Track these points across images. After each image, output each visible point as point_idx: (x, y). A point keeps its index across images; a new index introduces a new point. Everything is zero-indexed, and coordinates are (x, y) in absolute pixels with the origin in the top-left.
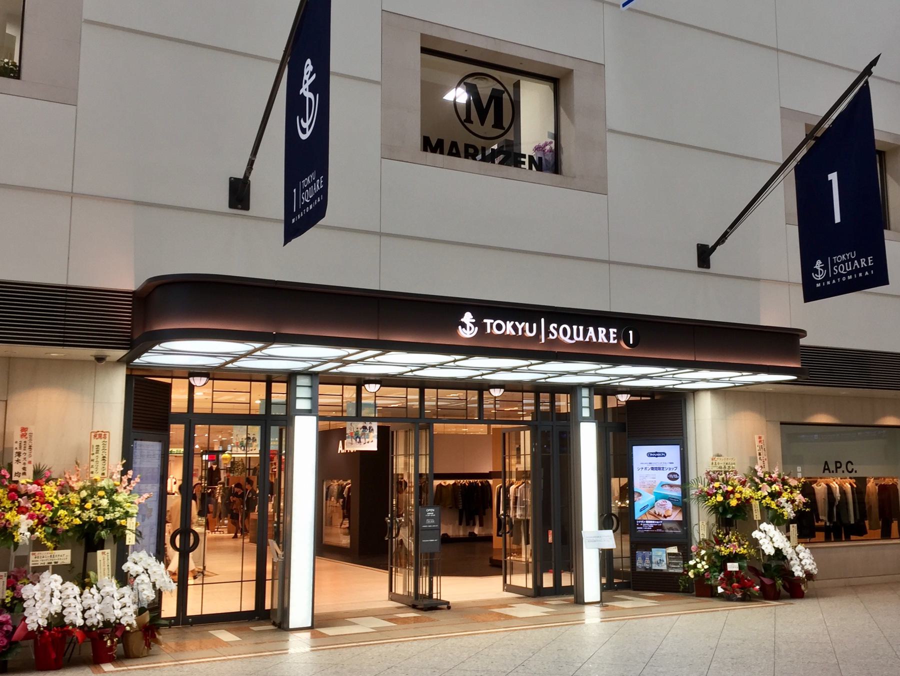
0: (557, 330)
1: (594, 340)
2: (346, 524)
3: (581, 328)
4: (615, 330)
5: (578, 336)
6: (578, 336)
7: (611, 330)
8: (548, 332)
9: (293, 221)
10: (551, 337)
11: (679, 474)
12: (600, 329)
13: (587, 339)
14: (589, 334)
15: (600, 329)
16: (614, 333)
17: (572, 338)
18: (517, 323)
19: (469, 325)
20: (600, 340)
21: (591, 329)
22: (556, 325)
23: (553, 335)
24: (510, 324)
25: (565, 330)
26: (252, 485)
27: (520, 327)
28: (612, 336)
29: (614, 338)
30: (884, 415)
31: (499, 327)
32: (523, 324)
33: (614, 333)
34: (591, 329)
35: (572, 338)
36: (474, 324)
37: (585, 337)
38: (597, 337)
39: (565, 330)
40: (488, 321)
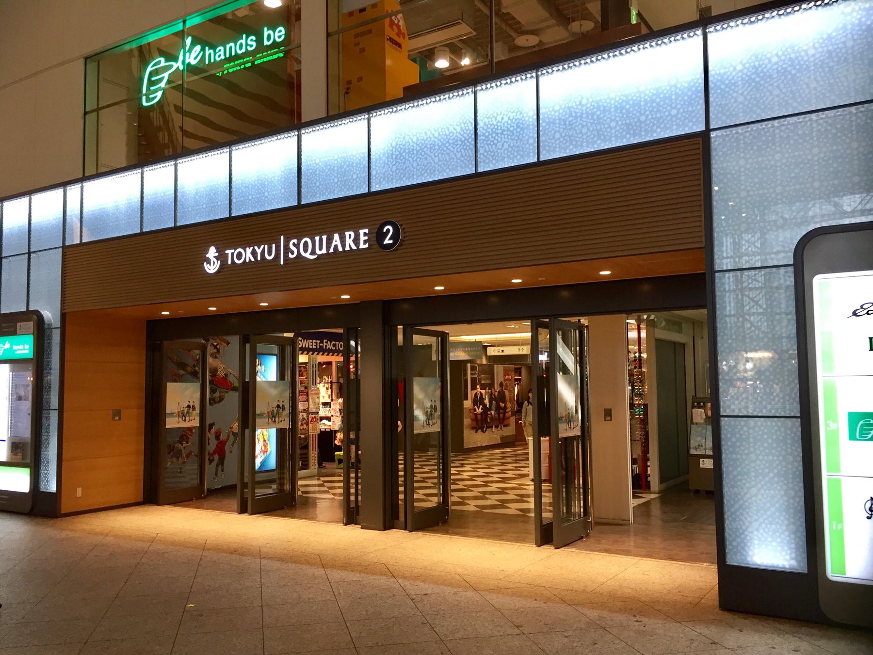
0: (297, 246)
1: (340, 249)
2: (341, 400)
3: (324, 237)
4: (367, 231)
5: (321, 249)
6: (321, 249)
7: (362, 232)
8: (287, 250)
9: (466, 62)
10: (291, 256)
11: (208, 356)
12: (347, 234)
13: (331, 251)
14: (334, 243)
15: (347, 234)
16: (365, 234)
17: (313, 252)
18: (256, 248)
19: (213, 260)
20: (347, 248)
21: (336, 236)
22: (295, 241)
23: (293, 253)
24: (249, 251)
25: (306, 243)
26: (643, 386)
27: (259, 251)
28: (363, 238)
29: (365, 242)
30: (47, 310)
31: (239, 256)
32: (262, 247)
33: (365, 234)
34: (336, 236)
35: (313, 252)
36: (217, 258)
37: (328, 248)
38: (343, 246)
39: (306, 243)
40: (229, 252)
